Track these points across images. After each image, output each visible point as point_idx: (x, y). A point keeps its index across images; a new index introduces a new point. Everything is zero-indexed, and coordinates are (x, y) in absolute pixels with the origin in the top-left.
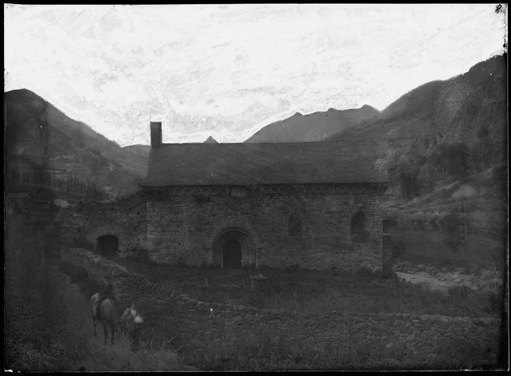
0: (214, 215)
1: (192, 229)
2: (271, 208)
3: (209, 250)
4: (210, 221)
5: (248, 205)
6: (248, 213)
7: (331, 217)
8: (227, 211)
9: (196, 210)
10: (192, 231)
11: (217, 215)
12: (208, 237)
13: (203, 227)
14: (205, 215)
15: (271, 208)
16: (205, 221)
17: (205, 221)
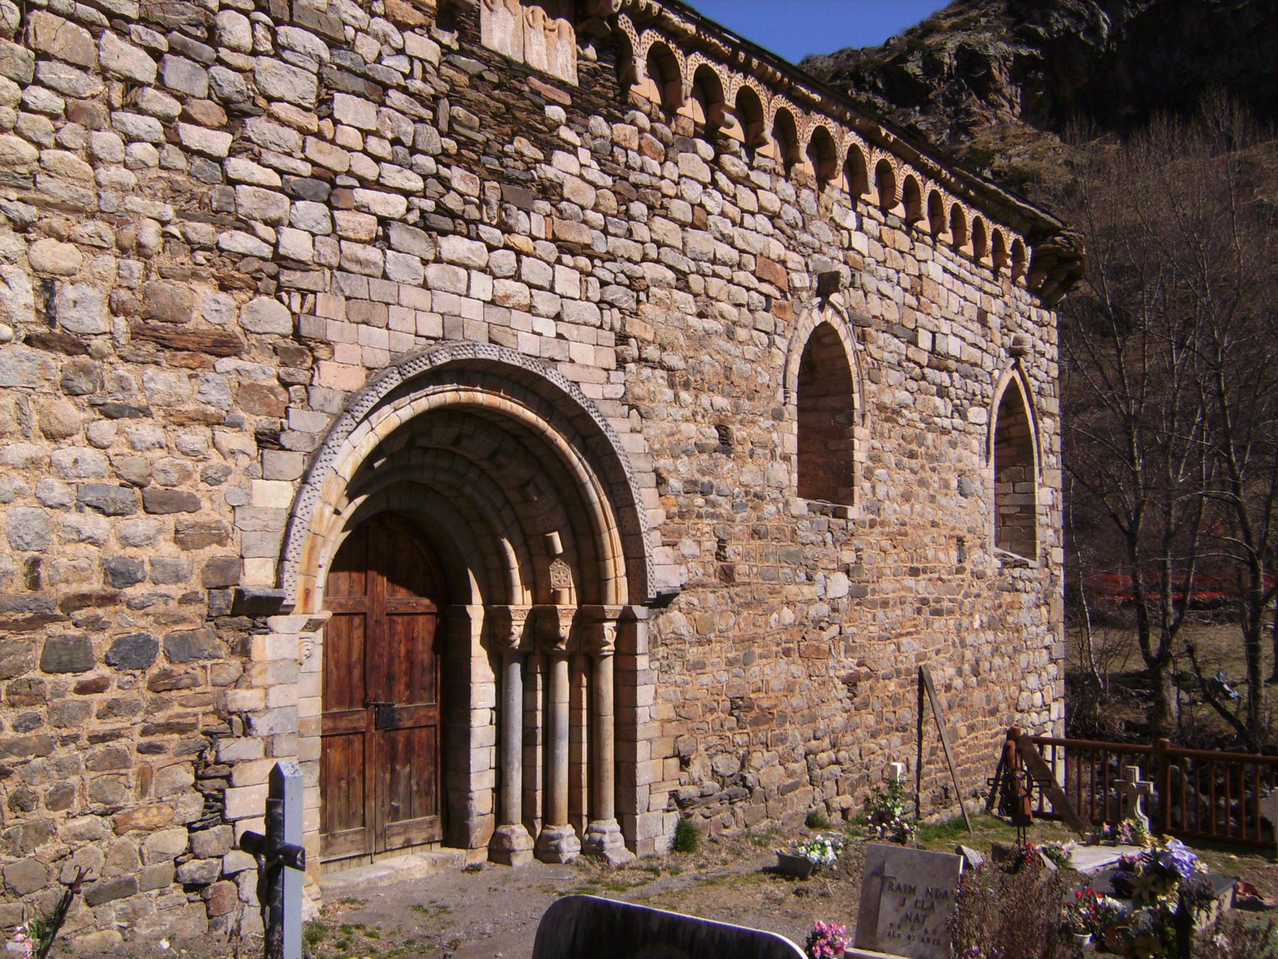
0: (329, 187)
1: (84, 310)
2: (724, 251)
3: (259, 609)
4: (295, 243)
5: (594, 173)
6: (585, 250)
7: (942, 392)
8: (446, 183)
9: (144, 68)
10: (74, 345)
11: (363, 195)
12: (268, 440)
13: (207, 306)
14: (240, 166)
15: (724, 251)
16: (237, 241)
17: (237, 241)
